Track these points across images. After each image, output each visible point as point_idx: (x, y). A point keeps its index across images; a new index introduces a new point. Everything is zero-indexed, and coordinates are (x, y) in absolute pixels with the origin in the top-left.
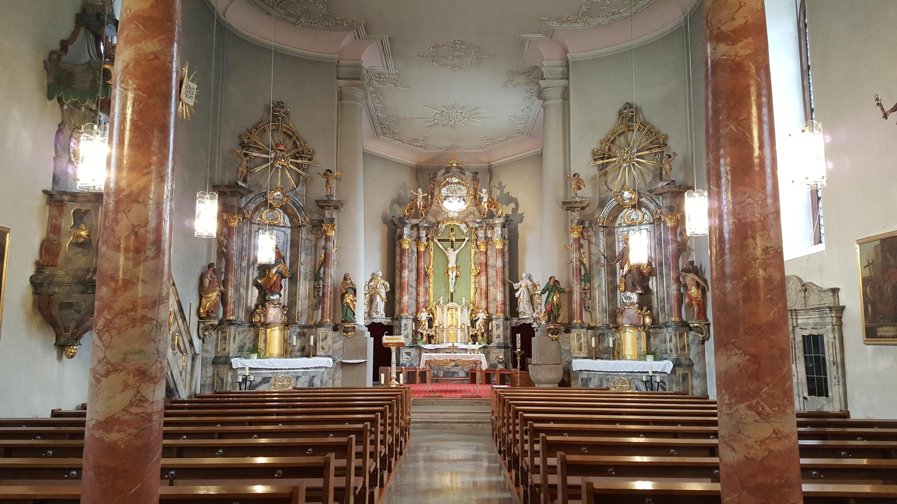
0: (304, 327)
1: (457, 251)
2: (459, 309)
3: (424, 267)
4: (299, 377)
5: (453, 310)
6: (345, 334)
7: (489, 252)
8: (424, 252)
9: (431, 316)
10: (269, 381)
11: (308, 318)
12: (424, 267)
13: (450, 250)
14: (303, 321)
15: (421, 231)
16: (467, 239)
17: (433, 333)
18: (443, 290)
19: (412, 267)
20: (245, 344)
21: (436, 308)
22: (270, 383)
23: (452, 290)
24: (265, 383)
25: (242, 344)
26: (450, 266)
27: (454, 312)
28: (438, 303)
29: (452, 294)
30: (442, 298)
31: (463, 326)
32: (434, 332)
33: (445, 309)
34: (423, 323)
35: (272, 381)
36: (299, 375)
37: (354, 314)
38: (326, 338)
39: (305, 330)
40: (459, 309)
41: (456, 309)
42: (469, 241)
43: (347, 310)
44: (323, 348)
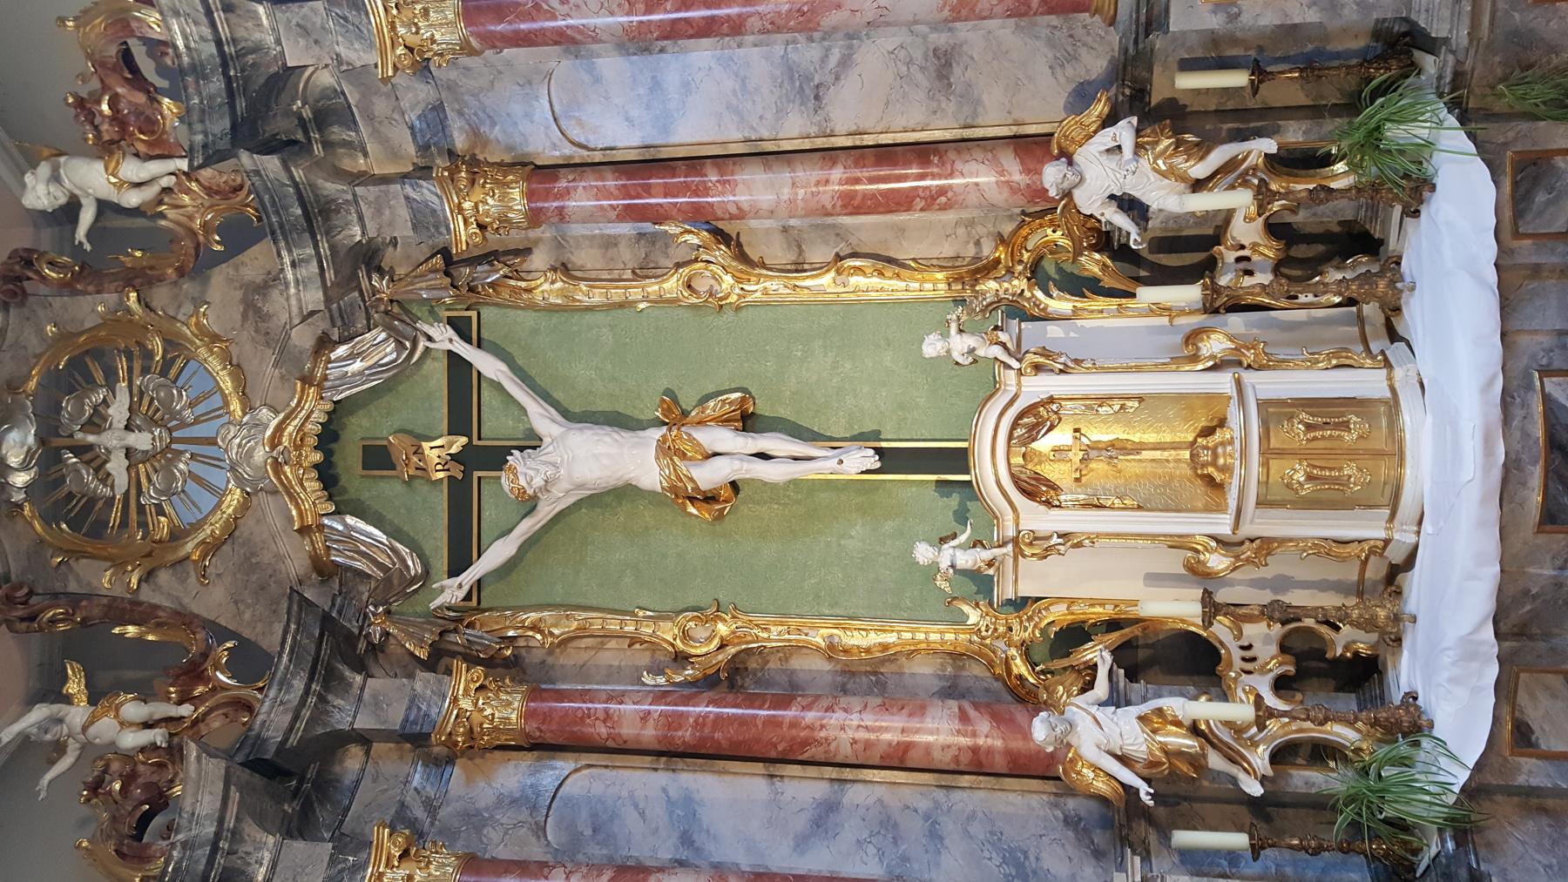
1: (541, 418)
2: (1037, 387)
3: (661, 696)
5: (1044, 444)
7: (546, 146)
8: (535, 694)
9: (1098, 653)
12: (661, 696)
13: (525, 472)
15: (364, 722)
16: (444, 338)
17: (1263, 636)
18: (857, 535)
19: (658, 811)
21: (1021, 603)
23: (859, 460)
26: (648, 472)
27: (1060, 436)
28: (980, 583)
29: (891, 460)
30: (924, 553)
31: (1215, 345)
32: (1254, 631)
33: (1036, 518)
34: (1189, 743)
40: (1037, 387)
41: (1035, 420)
42: (461, 328)
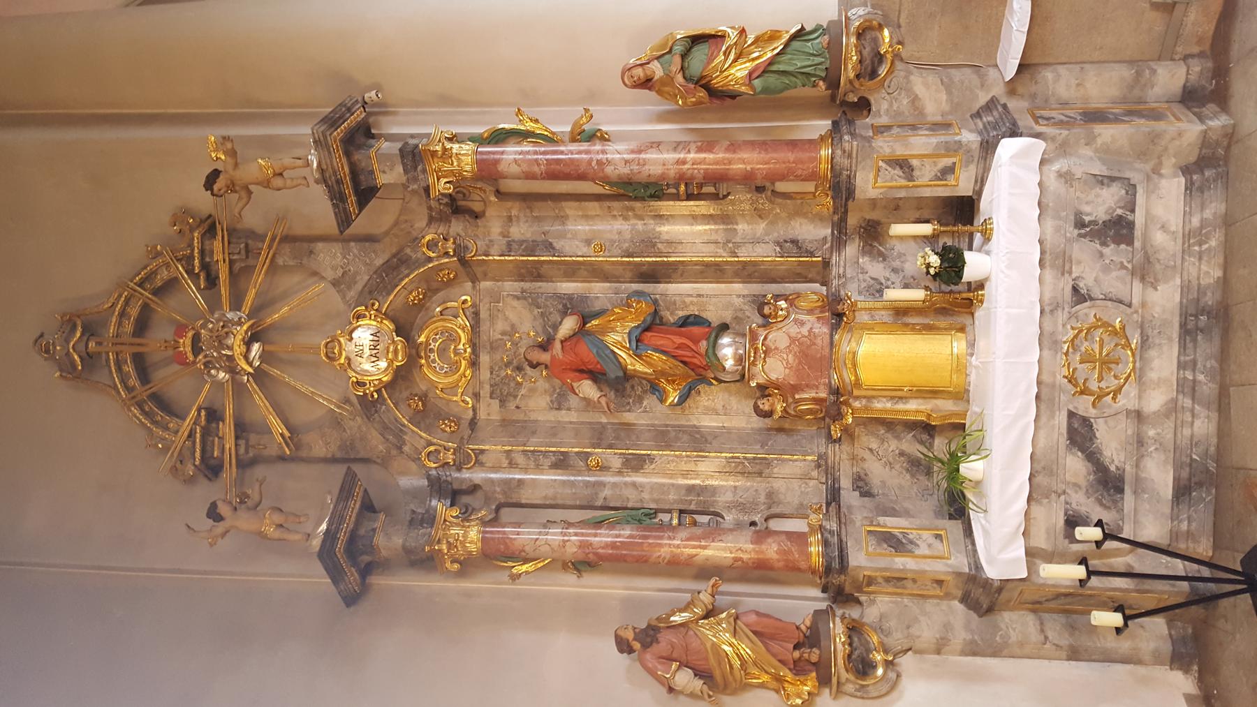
0: (840, 236)
4: (1075, 289)
6: (883, 71)
10: (1086, 421)
11: (805, 215)
14: (814, 231)
20: (902, 454)
22: (1092, 412)
24: (1092, 437)
25: (900, 464)
35: (1084, 406)
36: (1068, 289)
37: (800, 34)
38: (903, 165)
39: (853, 220)
43: (784, 73)
44: (949, 171)
